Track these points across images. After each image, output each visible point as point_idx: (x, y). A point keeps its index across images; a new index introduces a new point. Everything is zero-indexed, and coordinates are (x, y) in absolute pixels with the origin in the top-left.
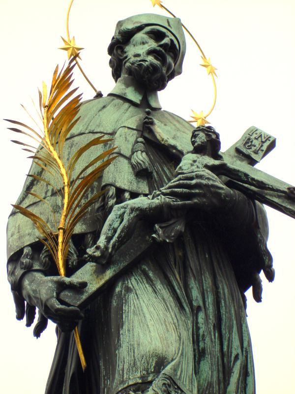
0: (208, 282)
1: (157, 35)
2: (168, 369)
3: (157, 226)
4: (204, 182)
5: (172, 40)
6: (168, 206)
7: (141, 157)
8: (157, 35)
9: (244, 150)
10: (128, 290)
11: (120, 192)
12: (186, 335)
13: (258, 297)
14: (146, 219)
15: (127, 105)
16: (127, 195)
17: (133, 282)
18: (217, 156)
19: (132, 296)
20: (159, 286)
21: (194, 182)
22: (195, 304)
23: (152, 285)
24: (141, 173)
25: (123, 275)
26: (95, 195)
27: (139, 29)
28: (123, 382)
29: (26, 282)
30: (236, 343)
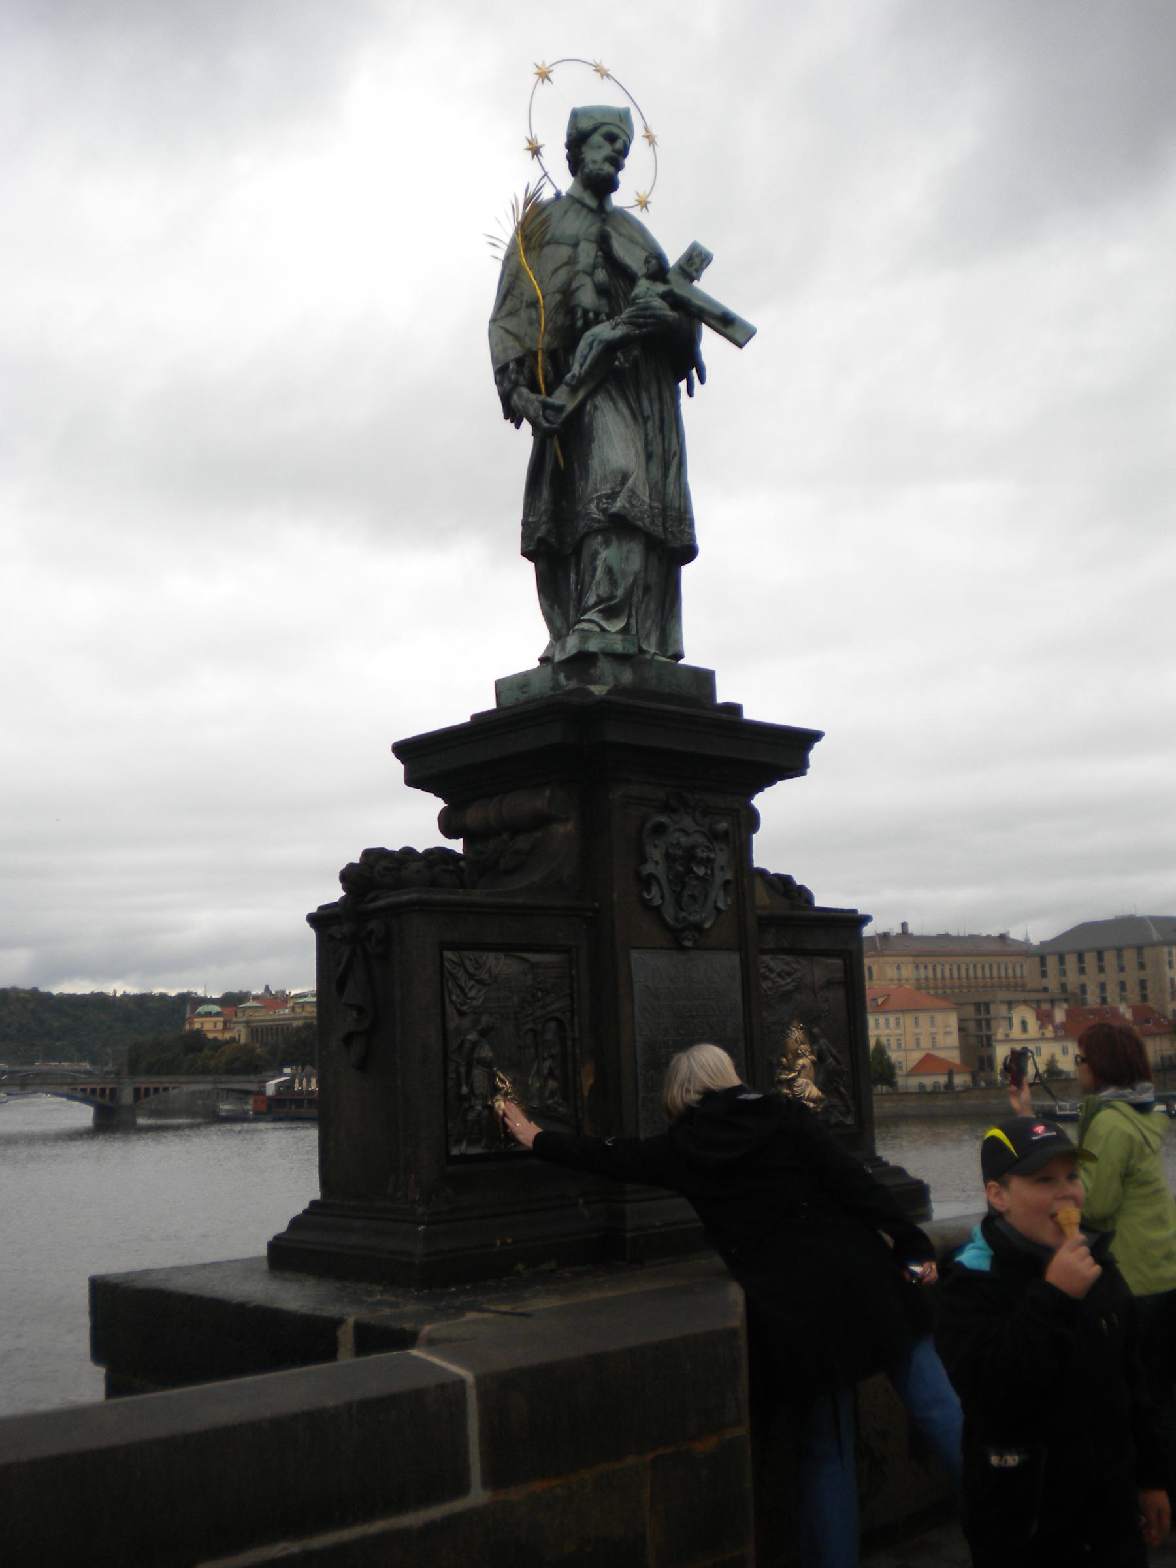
1: (611, 138)
2: (630, 482)
3: (619, 354)
7: (601, 275)
8: (611, 138)
9: (687, 269)
10: (596, 408)
11: (586, 312)
12: (640, 445)
13: (690, 392)
14: (610, 348)
15: (585, 211)
16: (591, 315)
17: (599, 400)
18: (665, 281)
19: (599, 413)
20: (621, 405)
23: (615, 404)
24: (602, 291)
25: (590, 395)
26: (570, 325)
27: (595, 129)
28: (596, 490)
29: (515, 397)
30: (674, 441)
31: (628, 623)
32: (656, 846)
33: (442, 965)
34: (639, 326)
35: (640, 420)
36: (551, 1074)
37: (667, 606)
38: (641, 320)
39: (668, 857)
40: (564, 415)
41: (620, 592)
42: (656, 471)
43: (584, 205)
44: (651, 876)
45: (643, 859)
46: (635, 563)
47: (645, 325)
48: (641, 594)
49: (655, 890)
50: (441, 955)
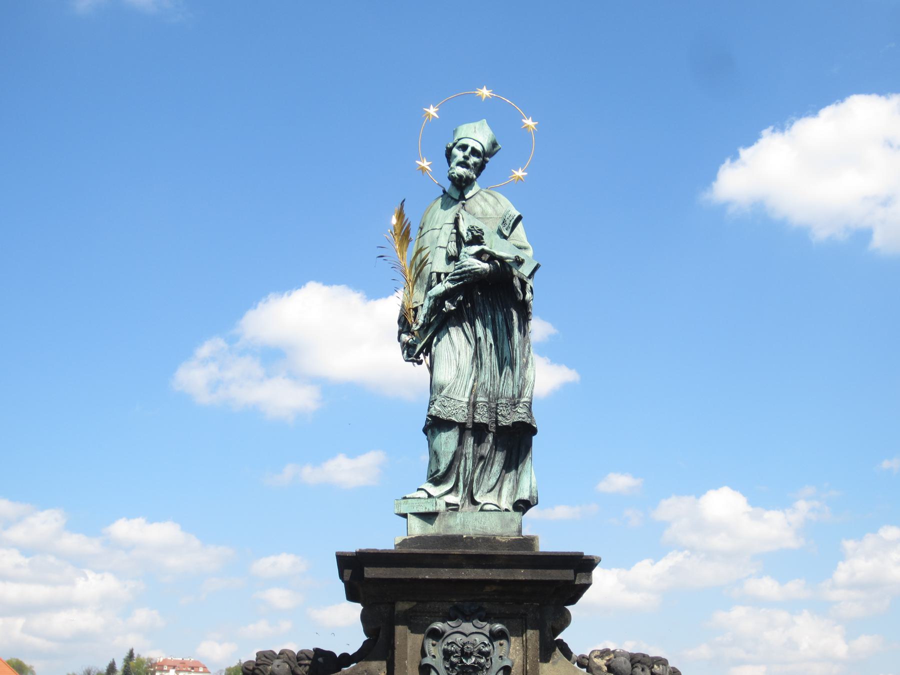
2: (444, 392)
3: (446, 303)
6: (451, 289)
7: (453, 248)
8: (464, 148)
11: (439, 275)
14: (439, 300)
18: (480, 243)
21: (460, 271)
27: (455, 144)
31: (456, 485)
32: (434, 645)
34: (458, 280)
35: (473, 342)
39: (447, 655)
41: (443, 468)
43: (452, 198)
45: (424, 654)
48: (470, 463)
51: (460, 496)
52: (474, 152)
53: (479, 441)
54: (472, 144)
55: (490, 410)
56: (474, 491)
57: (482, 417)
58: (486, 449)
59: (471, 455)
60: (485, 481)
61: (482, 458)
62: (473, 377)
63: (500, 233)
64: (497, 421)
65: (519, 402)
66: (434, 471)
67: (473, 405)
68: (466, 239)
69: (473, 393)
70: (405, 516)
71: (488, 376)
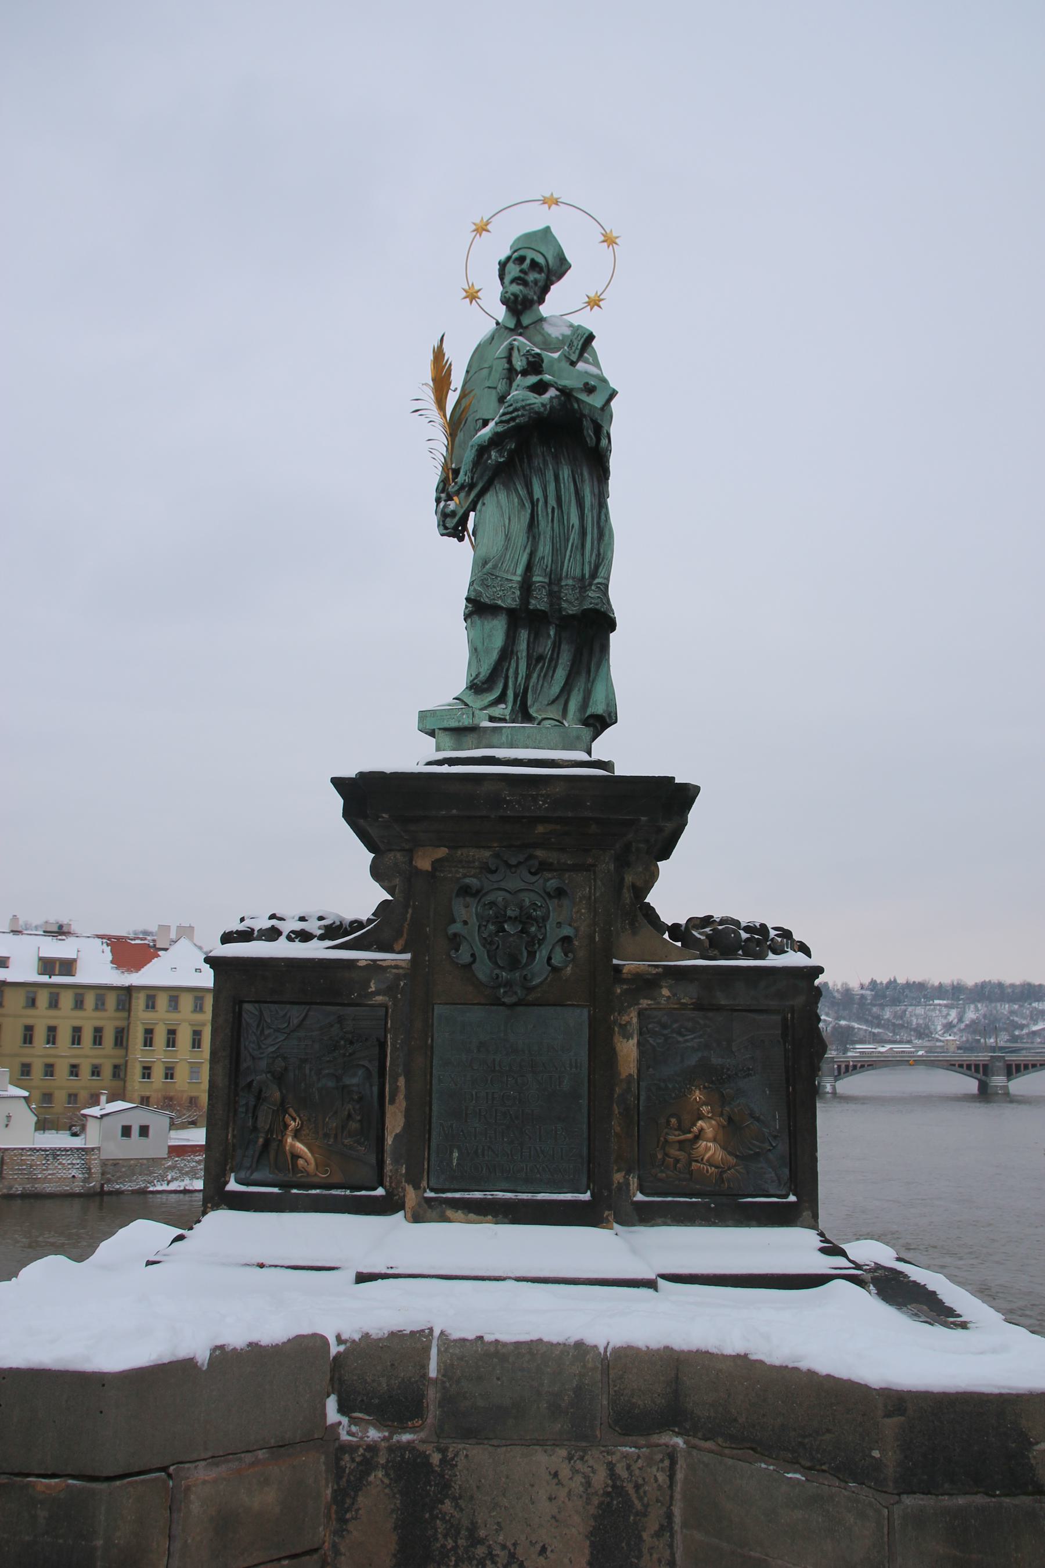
0: (550, 475)
3: (493, 453)
4: (519, 405)
5: (533, 261)
7: (501, 387)
8: (521, 260)
10: (484, 504)
12: (519, 527)
14: (482, 451)
19: (484, 508)
20: (503, 496)
22: (535, 498)
27: (509, 258)
33: (239, 1015)
34: (507, 422)
35: (528, 505)
36: (349, 1116)
37: (593, 669)
38: (508, 417)
40: (457, 518)
41: (485, 669)
42: (545, 549)
43: (507, 328)
44: (455, 935)
46: (498, 641)
47: (513, 419)
49: (464, 948)
50: (240, 1009)
51: (510, 708)
52: (534, 264)
53: (536, 635)
54: (530, 255)
55: (551, 594)
56: (529, 703)
57: (539, 602)
58: (546, 647)
59: (524, 654)
60: (545, 689)
61: (540, 658)
62: (528, 550)
63: (568, 358)
64: (560, 610)
65: (590, 584)
66: (474, 675)
67: (526, 586)
68: (519, 369)
69: (529, 568)
70: (432, 734)
71: (548, 548)
